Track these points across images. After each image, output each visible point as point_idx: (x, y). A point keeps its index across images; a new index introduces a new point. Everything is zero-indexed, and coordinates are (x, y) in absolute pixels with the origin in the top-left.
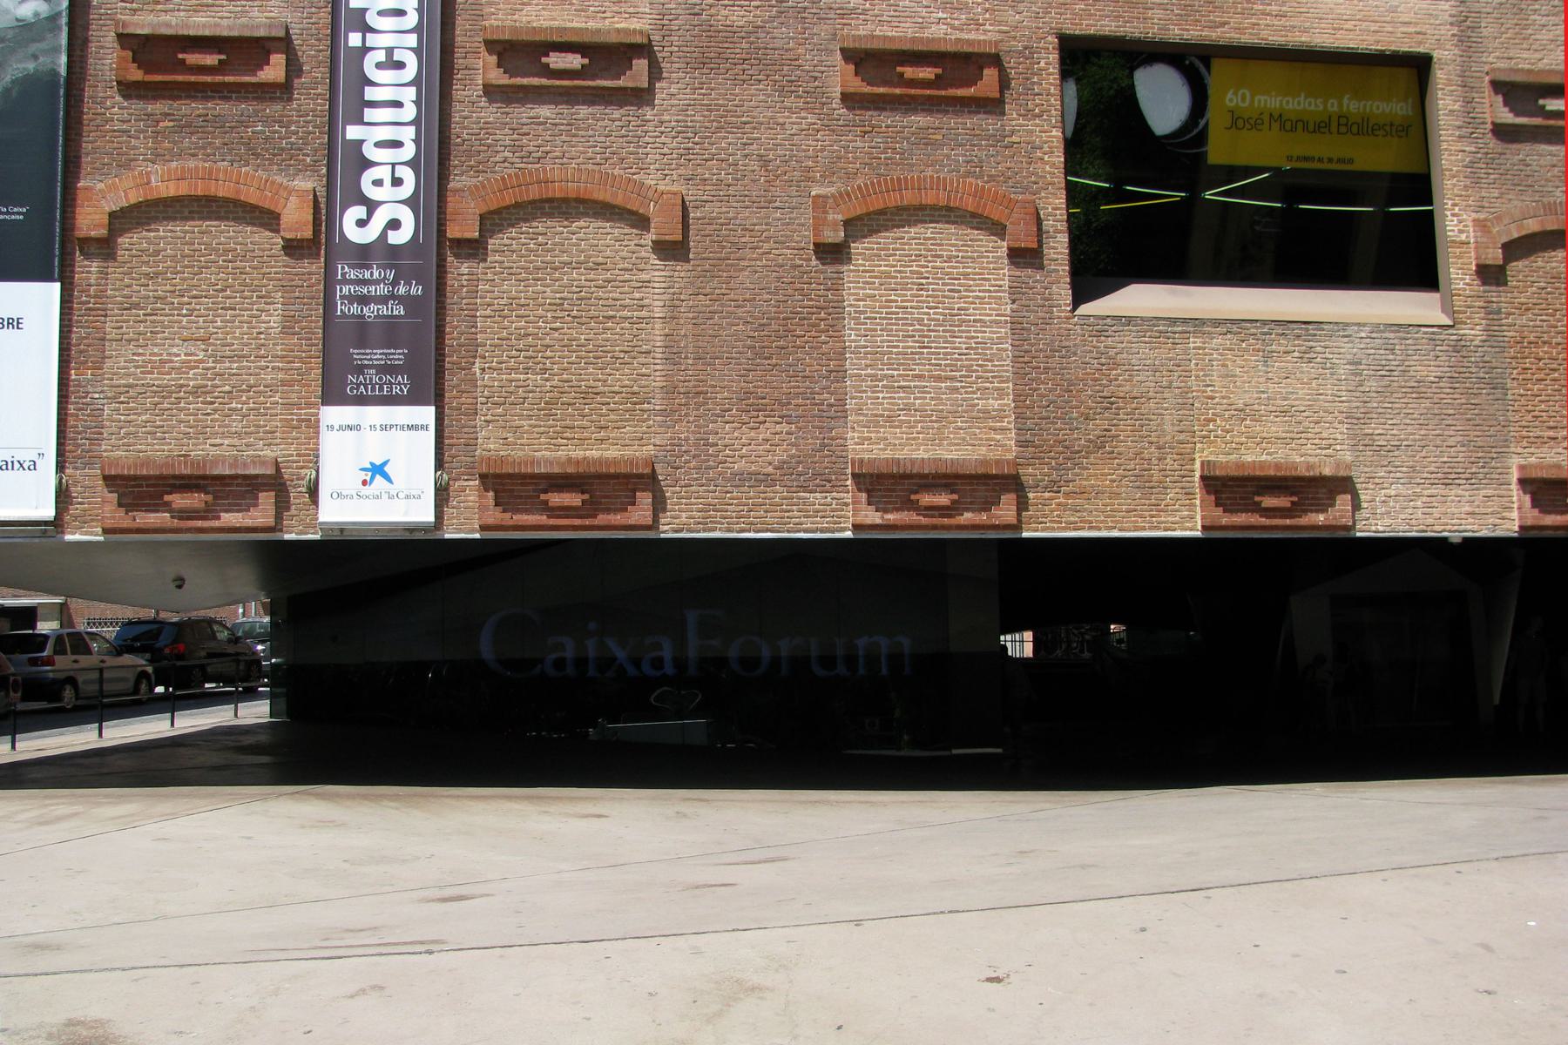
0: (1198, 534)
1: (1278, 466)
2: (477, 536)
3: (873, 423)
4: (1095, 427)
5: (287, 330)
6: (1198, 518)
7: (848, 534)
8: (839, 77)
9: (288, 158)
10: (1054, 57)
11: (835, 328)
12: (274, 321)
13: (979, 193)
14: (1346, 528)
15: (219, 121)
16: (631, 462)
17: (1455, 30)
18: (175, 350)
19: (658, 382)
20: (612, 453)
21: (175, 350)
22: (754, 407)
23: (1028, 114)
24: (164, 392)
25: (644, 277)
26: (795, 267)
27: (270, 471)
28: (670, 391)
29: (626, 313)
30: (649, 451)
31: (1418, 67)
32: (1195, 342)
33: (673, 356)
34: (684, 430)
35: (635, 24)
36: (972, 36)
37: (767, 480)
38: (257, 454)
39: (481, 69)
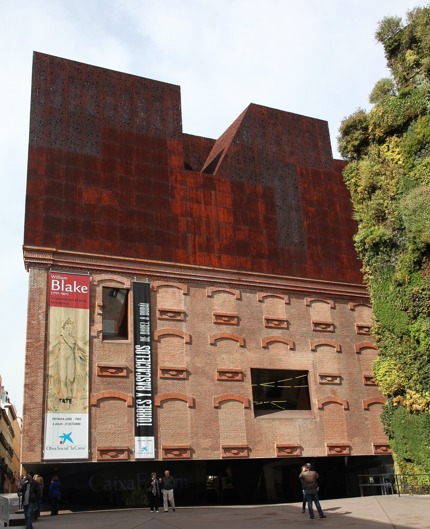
0: (276, 457)
1: (288, 445)
2: (162, 460)
3: (224, 438)
4: (258, 439)
5: (128, 422)
6: (276, 454)
7: (221, 459)
8: (216, 376)
9: (127, 389)
10: (250, 372)
11: (217, 421)
12: (126, 419)
13: (239, 397)
14: (299, 456)
15: (115, 382)
16: (187, 446)
17: (312, 366)
18: (109, 426)
19: (190, 431)
20: (183, 445)
21: (109, 426)
22: (205, 436)
23: (246, 382)
24: (107, 434)
25: (187, 412)
26: (210, 411)
27: (127, 449)
28: (192, 433)
29: (184, 419)
30: (189, 444)
31: (306, 372)
32: (274, 423)
33: (192, 427)
34: (194, 440)
35: (183, 366)
36: (236, 369)
37: (208, 449)
38: (124, 445)
39: (160, 374)
